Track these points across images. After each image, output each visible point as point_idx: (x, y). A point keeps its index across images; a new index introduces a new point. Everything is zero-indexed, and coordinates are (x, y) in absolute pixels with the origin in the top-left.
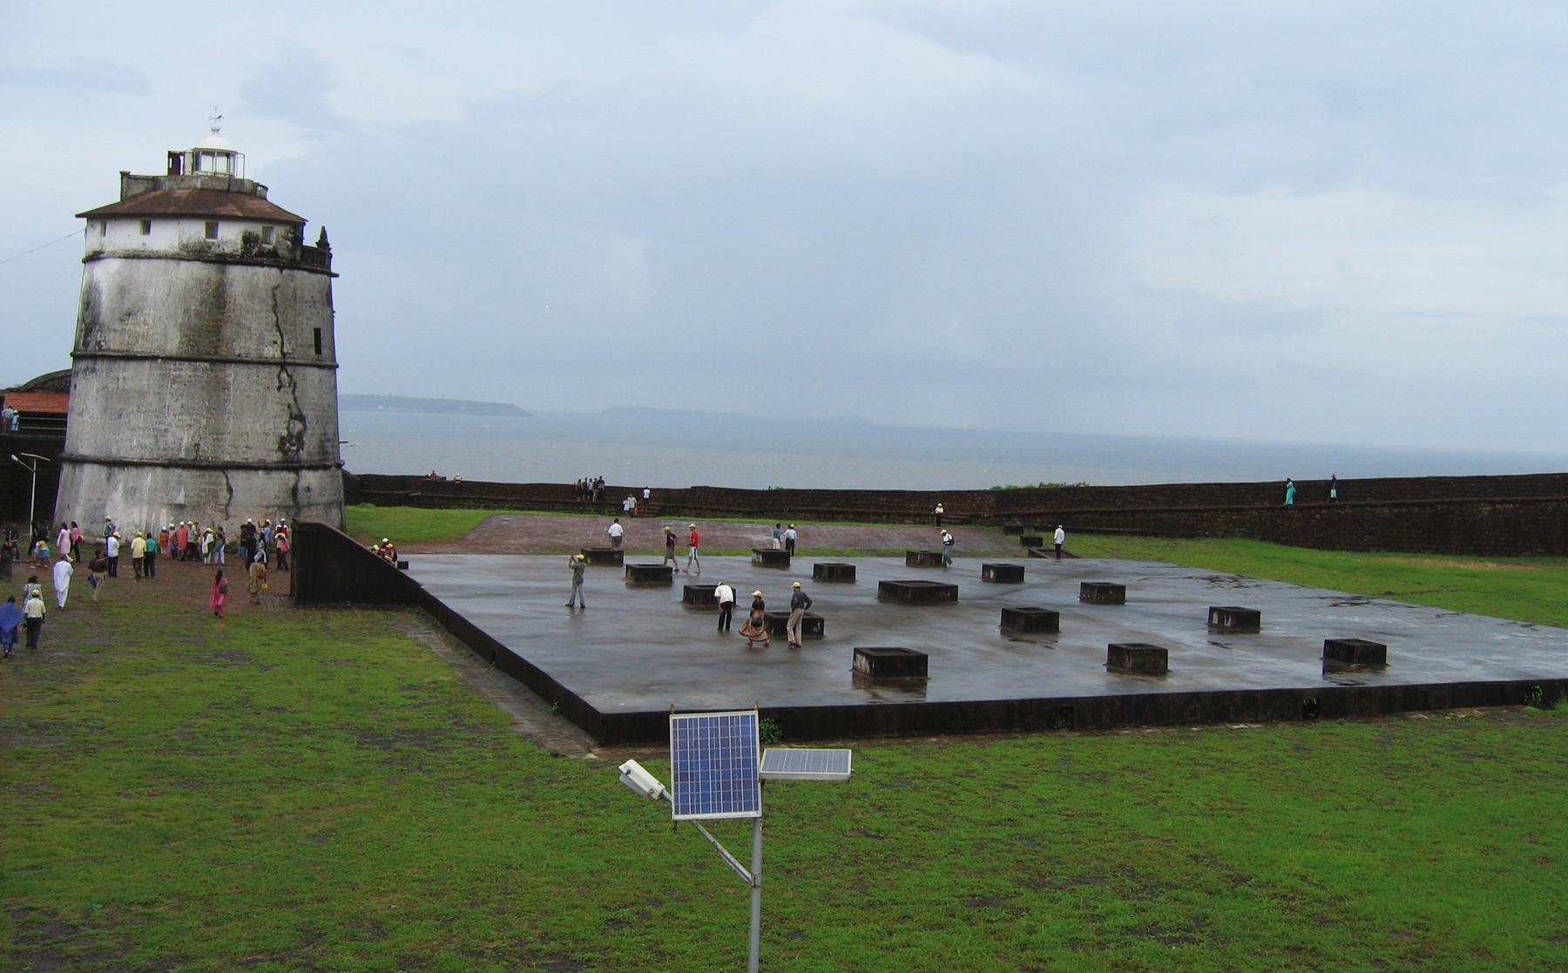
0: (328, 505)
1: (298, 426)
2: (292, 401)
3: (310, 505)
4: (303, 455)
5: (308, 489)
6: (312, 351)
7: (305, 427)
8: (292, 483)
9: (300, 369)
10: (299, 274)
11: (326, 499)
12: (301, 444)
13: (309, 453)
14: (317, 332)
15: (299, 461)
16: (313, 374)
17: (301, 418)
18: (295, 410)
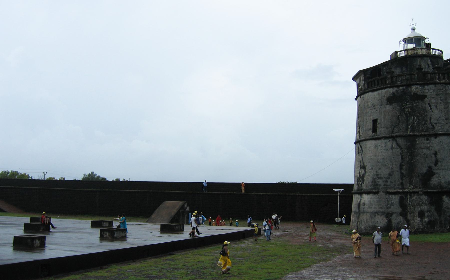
0: (375, 214)
1: (363, 171)
2: (361, 159)
3: (364, 212)
4: (364, 186)
5: (364, 204)
6: (370, 132)
7: (365, 171)
8: (359, 200)
9: (364, 143)
10: (366, 95)
11: (372, 210)
12: (363, 181)
13: (367, 186)
14: (375, 122)
15: (362, 189)
16: (371, 144)
17: (363, 167)
18: (362, 164)
